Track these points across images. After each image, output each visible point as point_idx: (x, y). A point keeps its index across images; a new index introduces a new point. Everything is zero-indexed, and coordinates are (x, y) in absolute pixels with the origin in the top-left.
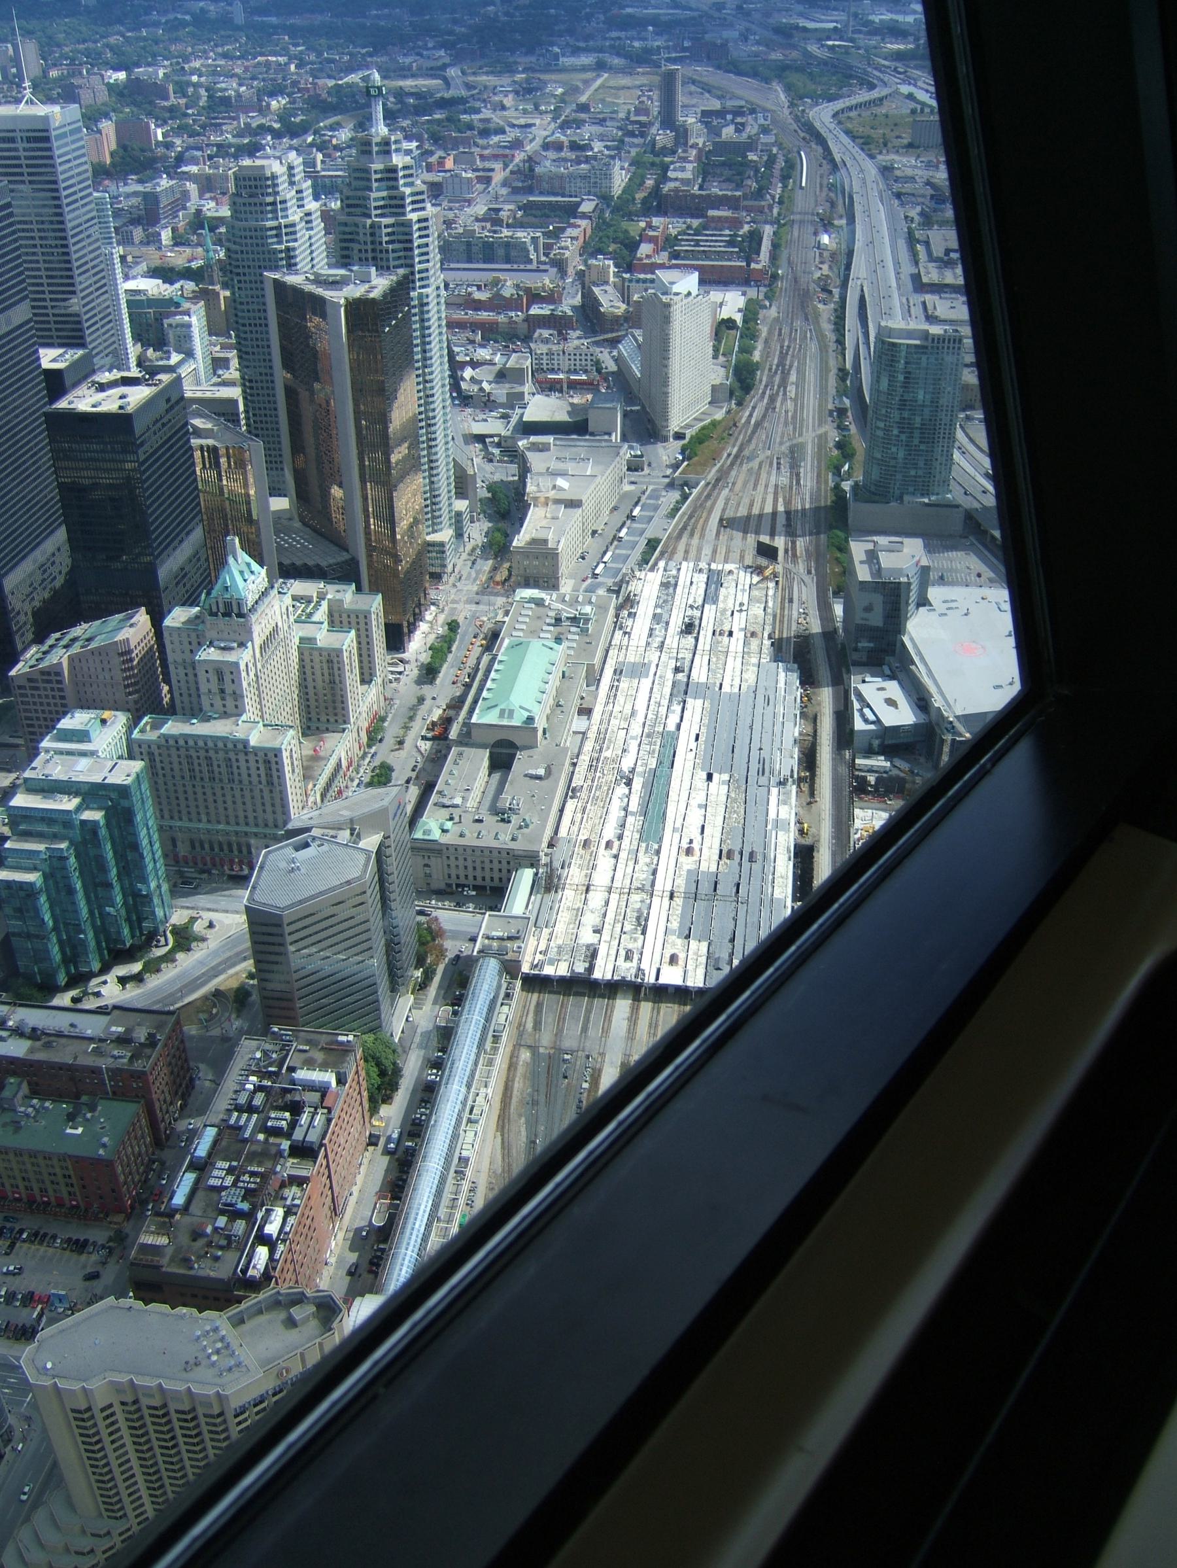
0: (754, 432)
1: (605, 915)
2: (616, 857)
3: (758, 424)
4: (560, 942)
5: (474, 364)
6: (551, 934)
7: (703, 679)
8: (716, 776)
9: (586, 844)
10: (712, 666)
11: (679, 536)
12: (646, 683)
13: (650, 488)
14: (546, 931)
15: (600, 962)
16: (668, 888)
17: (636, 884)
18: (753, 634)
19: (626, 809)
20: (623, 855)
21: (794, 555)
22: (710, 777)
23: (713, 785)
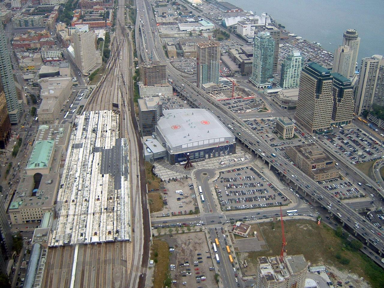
0: (110, 71)
1: (73, 224)
2: (76, 204)
3: (111, 68)
4: (59, 234)
5: (23, 57)
6: (57, 232)
7: (99, 146)
8: (105, 175)
9: (66, 202)
10: (102, 142)
11: (90, 104)
12: (82, 149)
13: (80, 90)
14: (55, 232)
15: (73, 238)
16: (93, 212)
17: (83, 212)
18: (113, 131)
19: (78, 189)
20: (78, 204)
21: (124, 106)
22: (103, 176)
23: (104, 178)
